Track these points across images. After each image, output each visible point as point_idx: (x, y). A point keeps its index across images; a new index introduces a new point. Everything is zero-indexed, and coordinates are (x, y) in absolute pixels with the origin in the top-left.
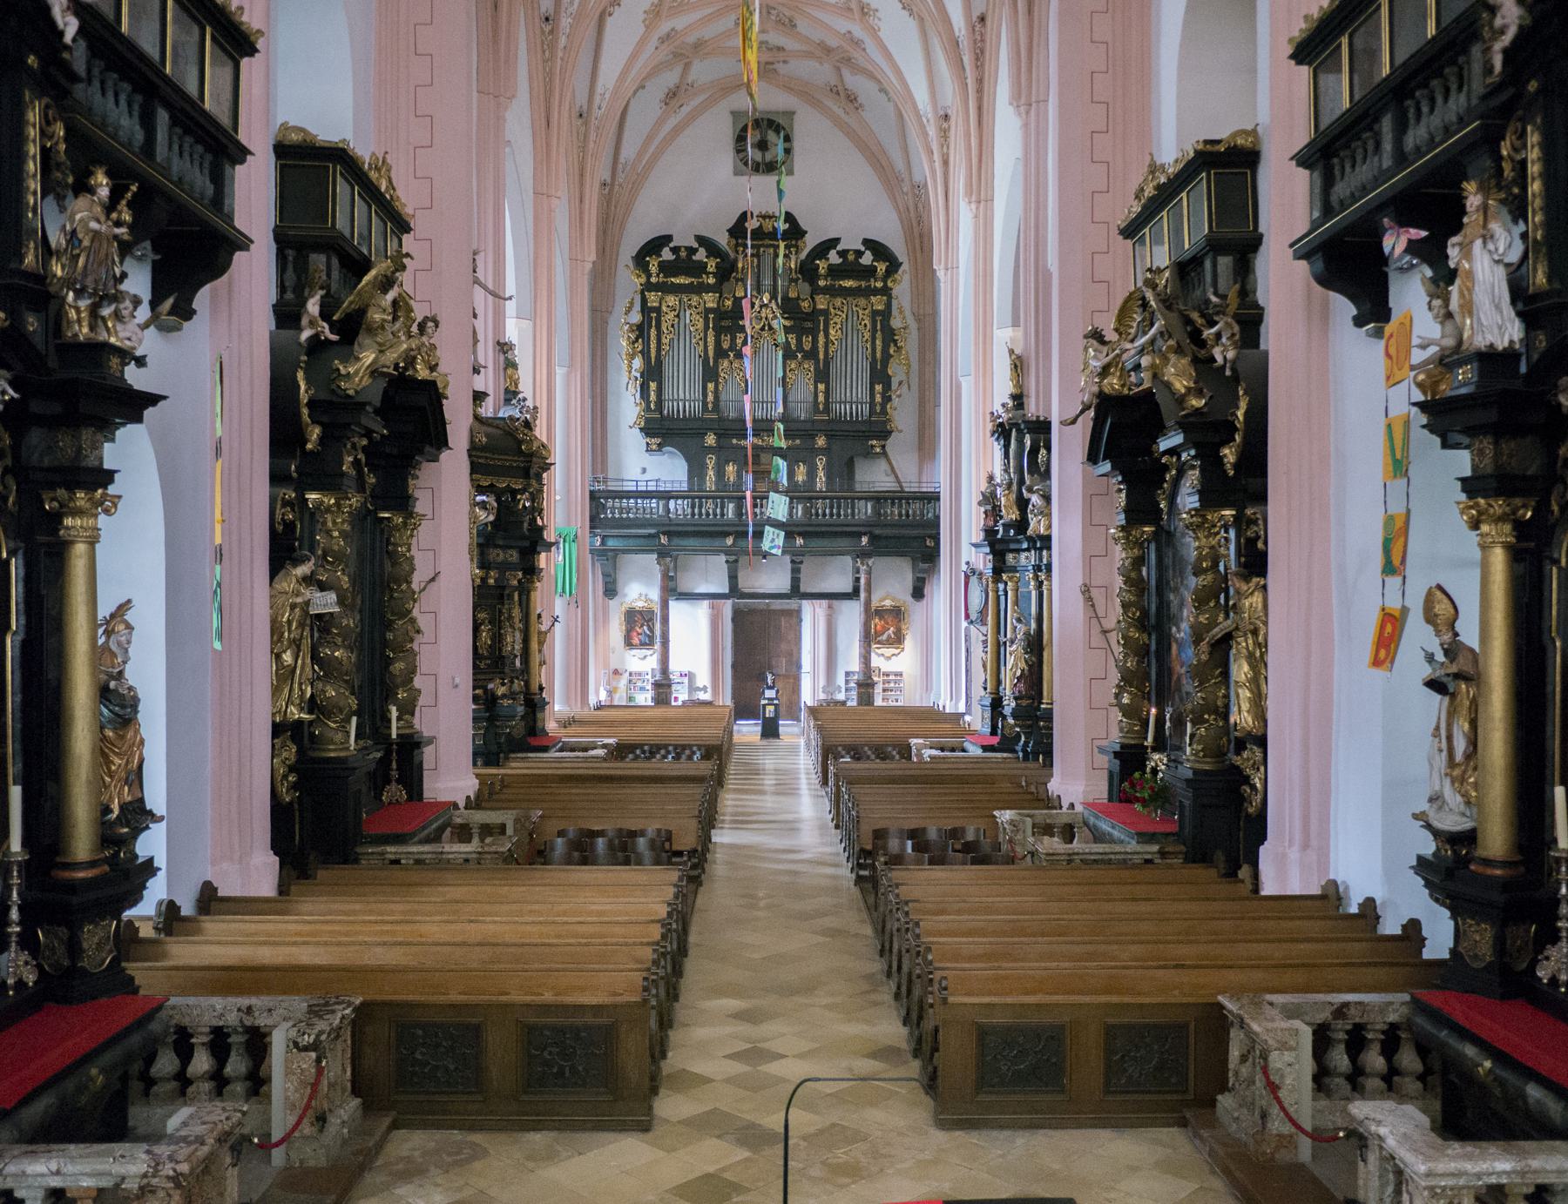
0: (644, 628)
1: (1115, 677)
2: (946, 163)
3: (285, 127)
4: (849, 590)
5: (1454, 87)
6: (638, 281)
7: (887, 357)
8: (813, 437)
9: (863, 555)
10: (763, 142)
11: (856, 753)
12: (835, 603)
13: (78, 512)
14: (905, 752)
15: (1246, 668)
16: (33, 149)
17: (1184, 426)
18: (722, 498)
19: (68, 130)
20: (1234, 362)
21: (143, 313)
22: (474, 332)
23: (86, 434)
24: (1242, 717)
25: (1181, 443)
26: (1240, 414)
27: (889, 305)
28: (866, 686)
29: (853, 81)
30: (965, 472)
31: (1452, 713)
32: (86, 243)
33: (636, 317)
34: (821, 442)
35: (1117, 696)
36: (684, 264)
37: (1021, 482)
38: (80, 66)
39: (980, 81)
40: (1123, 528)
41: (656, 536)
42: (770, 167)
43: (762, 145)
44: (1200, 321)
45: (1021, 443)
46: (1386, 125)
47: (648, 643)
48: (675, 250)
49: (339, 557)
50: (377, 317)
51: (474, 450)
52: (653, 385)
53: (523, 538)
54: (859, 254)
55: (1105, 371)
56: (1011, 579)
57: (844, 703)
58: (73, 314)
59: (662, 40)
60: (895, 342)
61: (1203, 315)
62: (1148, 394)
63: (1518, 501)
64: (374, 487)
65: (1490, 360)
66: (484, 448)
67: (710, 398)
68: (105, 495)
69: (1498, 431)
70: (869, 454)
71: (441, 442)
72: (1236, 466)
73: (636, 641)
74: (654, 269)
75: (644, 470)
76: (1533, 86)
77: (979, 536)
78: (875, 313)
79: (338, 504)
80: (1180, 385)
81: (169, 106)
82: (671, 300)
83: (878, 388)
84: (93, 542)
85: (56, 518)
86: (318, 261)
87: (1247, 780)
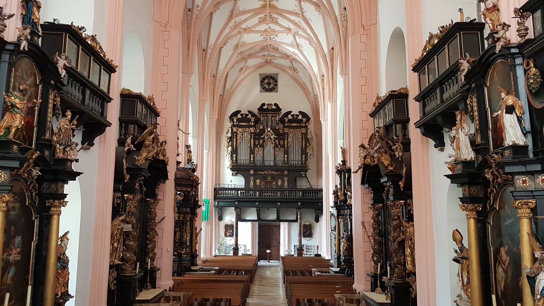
0: (231, 231)
1: (372, 251)
2: (323, 89)
3: (124, 89)
4: (295, 219)
5: (455, 82)
7: (306, 147)
8: (283, 171)
9: (299, 208)
10: (269, 83)
11: (295, 273)
12: (291, 223)
13: (56, 206)
14: (310, 273)
15: (409, 251)
16: (51, 106)
17: (387, 175)
18: (255, 190)
19: (61, 99)
20: (401, 156)
21: (80, 146)
22: (178, 144)
23: (60, 184)
24: (409, 266)
25: (387, 181)
26: (404, 172)
27: (307, 131)
28: (300, 250)
29: (295, 65)
30: (329, 183)
31: (462, 270)
32: (63, 131)
33: (229, 135)
34: (286, 173)
35: (372, 257)
36: (245, 118)
37: (345, 188)
38: (65, 82)
39: (332, 66)
40: (372, 205)
41: (235, 202)
42: (271, 90)
43: (269, 84)
44: (392, 144)
45: (345, 176)
46: (438, 91)
47: (232, 236)
48: (242, 115)
49: (133, 214)
50: (148, 143)
51: (176, 179)
52: (234, 155)
53: (192, 204)
54: (298, 116)
55: (365, 157)
56: (342, 218)
57: (293, 255)
58: (58, 151)
59: (238, 54)
61: (392, 142)
62: (377, 165)
63: (477, 205)
64: (146, 191)
65: (466, 164)
66: (180, 178)
67: (252, 159)
68: (64, 202)
69: (470, 184)
70: (301, 176)
71: (166, 178)
72: (403, 188)
73: (228, 235)
74: (235, 121)
75: (231, 181)
76: (473, 85)
77: (332, 204)
78: (302, 133)
79: (133, 198)
80: (386, 163)
81: (90, 89)
82: (240, 130)
84: (59, 215)
85: (49, 208)
86: (131, 127)
87: (411, 286)
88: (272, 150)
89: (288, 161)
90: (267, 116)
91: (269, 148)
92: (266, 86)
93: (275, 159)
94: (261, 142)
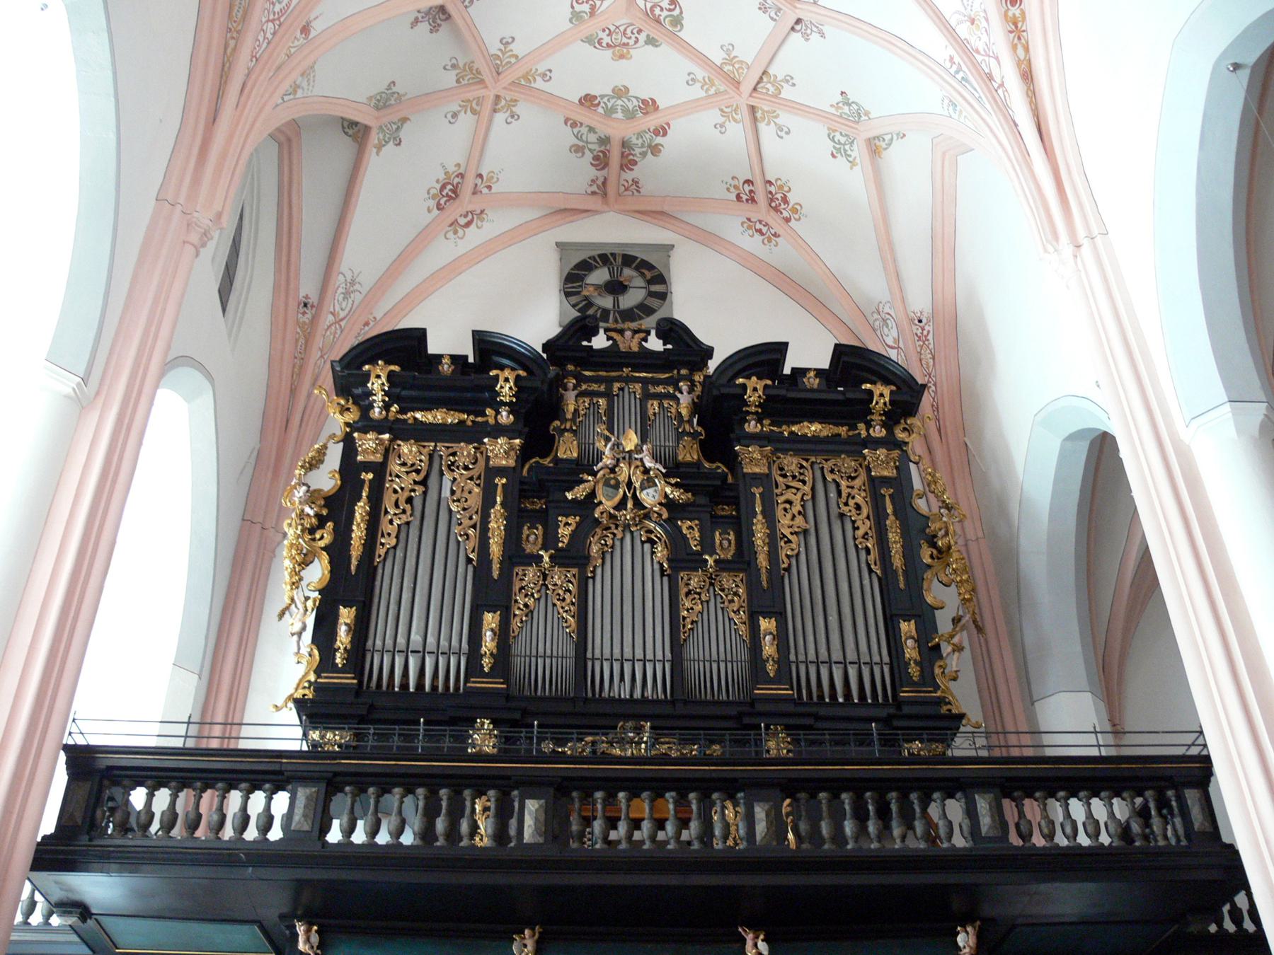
6: (337, 421)
7: (915, 571)
27: (903, 471)
33: (326, 479)
52: (346, 615)
67: (489, 642)
74: (377, 385)
82: (407, 449)
88: (654, 590)
90: (608, 395)
93: (677, 646)
94: (565, 532)
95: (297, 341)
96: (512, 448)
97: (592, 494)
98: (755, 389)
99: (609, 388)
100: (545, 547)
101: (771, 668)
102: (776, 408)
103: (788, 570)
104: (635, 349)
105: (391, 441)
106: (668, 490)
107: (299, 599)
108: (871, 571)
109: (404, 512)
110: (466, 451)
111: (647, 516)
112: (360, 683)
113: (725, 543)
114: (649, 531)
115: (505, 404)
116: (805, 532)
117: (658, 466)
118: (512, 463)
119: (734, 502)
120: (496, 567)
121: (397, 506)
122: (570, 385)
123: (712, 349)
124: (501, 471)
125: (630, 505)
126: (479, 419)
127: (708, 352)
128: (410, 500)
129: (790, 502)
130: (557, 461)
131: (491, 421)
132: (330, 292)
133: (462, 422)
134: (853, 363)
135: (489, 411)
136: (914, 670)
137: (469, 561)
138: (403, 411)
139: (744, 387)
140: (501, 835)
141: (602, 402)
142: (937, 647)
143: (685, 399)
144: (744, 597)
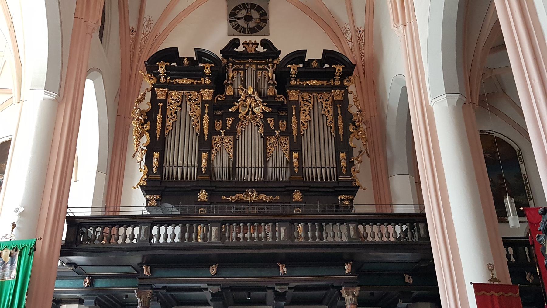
33: (146, 106)
43: (248, 18)
52: (156, 155)
60: (353, 123)
67: (204, 163)
74: (162, 71)
78: (335, 103)
82: (174, 94)
83: (342, 155)
88: (259, 143)
89: (300, 167)
90: (244, 69)
91: (251, 139)
92: (242, 23)
93: (266, 162)
94: (229, 123)
95: (131, 45)
96: (210, 93)
97: (238, 110)
98: (294, 69)
99: (244, 67)
100: (222, 129)
101: (296, 170)
102: (302, 75)
103: (303, 135)
104: (253, 52)
105: (168, 91)
106: (263, 108)
107: (139, 150)
108: (331, 135)
109: (174, 117)
110: (194, 94)
111: (256, 117)
112: (162, 178)
113: (283, 126)
114: (257, 122)
115: (207, 76)
116: (310, 121)
117: (260, 99)
118: (210, 98)
119: (286, 110)
120: (206, 136)
121: (172, 115)
122: (230, 66)
123: (280, 51)
124: (207, 102)
125: (250, 113)
126: (198, 82)
127: (279, 52)
128: (176, 113)
129: (305, 110)
130: (226, 96)
131: (203, 82)
132: (141, 25)
133: (193, 83)
134: (329, 56)
135: (202, 79)
136: (344, 170)
137: (197, 134)
138: (171, 79)
139: (290, 68)
140: (204, 238)
141: (242, 72)
142: (353, 161)
143: (270, 70)
144: (288, 145)
